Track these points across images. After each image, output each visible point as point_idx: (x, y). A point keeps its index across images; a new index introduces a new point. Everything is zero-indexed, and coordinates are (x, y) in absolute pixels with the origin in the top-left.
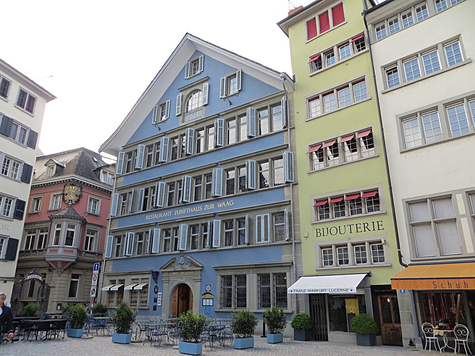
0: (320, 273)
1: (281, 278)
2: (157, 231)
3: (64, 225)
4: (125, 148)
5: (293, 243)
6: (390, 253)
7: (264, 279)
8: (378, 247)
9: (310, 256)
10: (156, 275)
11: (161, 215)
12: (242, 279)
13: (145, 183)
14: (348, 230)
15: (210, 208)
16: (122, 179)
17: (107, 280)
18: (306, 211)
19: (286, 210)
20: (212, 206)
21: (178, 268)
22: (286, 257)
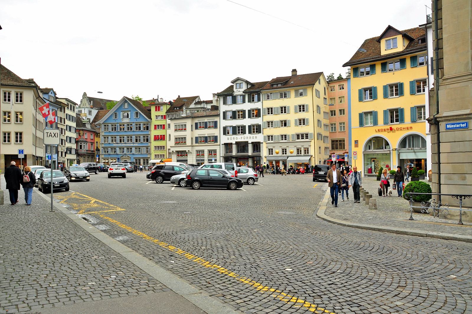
0: (154, 159)
1: (147, 160)
2: (118, 149)
3: (83, 143)
4: (103, 123)
5: (150, 154)
6: (165, 156)
7: (144, 160)
8: (164, 155)
9: (153, 156)
10: (118, 159)
11: (118, 144)
12: (140, 160)
13: (112, 136)
14: (159, 153)
15: (132, 145)
16: (104, 133)
17: (103, 159)
18: (153, 148)
19: (149, 148)
20: (132, 144)
21: (125, 157)
22: (148, 156)
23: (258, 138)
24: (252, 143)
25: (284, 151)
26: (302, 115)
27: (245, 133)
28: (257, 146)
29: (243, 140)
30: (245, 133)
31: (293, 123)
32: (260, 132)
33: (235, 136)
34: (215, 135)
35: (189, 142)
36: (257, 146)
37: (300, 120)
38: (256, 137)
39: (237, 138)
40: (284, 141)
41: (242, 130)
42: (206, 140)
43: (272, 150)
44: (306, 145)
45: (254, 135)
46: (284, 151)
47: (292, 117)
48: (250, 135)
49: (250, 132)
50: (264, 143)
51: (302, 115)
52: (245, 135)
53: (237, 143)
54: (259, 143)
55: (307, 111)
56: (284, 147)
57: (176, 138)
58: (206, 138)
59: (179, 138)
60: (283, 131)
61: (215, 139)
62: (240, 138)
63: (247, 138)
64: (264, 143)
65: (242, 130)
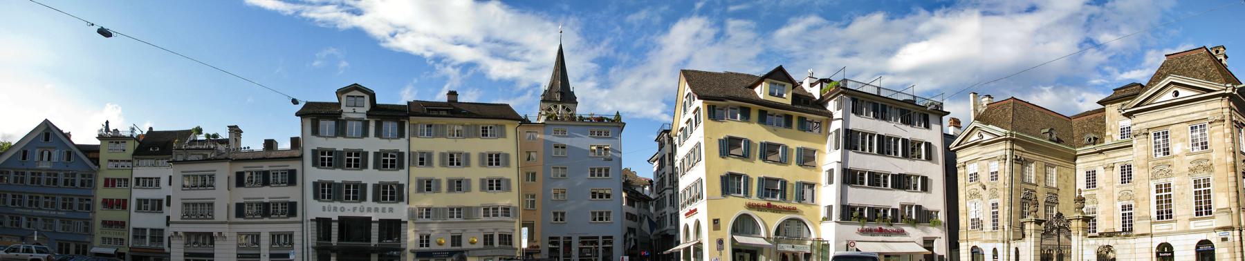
23: (398, 211)
24: (382, 222)
25: (456, 240)
26: (495, 172)
27: (364, 198)
28: (392, 228)
29: (358, 214)
30: (364, 198)
31: (476, 185)
32: (401, 199)
33: (338, 204)
34: (291, 200)
35: (220, 213)
36: (392, 228)
37: (491, 181)
38: (391, 210)
39: (343, 209)
40: (455, 219)
41: (356, 192)
42: (266, 210)
43: (428, 237)
44: (506, 230)
45: (387, 206)
46: (456, 240)
47: (475, 173)
48: (376, 205)
49: (376, 199)
50: (410, 223)
51: (495, 172)
52: (363, 203)
53: (342, 220)
54: (398, 223)
55: (507, 164)
56: (456, 231)
57: (186, 205)
58: (267, 205)
59: (195, 205)
60: (458, 199)
61: (291, 209)
62: (351, 209)
63: (369, 210)
64: (410, 223)
65: (356, 192)
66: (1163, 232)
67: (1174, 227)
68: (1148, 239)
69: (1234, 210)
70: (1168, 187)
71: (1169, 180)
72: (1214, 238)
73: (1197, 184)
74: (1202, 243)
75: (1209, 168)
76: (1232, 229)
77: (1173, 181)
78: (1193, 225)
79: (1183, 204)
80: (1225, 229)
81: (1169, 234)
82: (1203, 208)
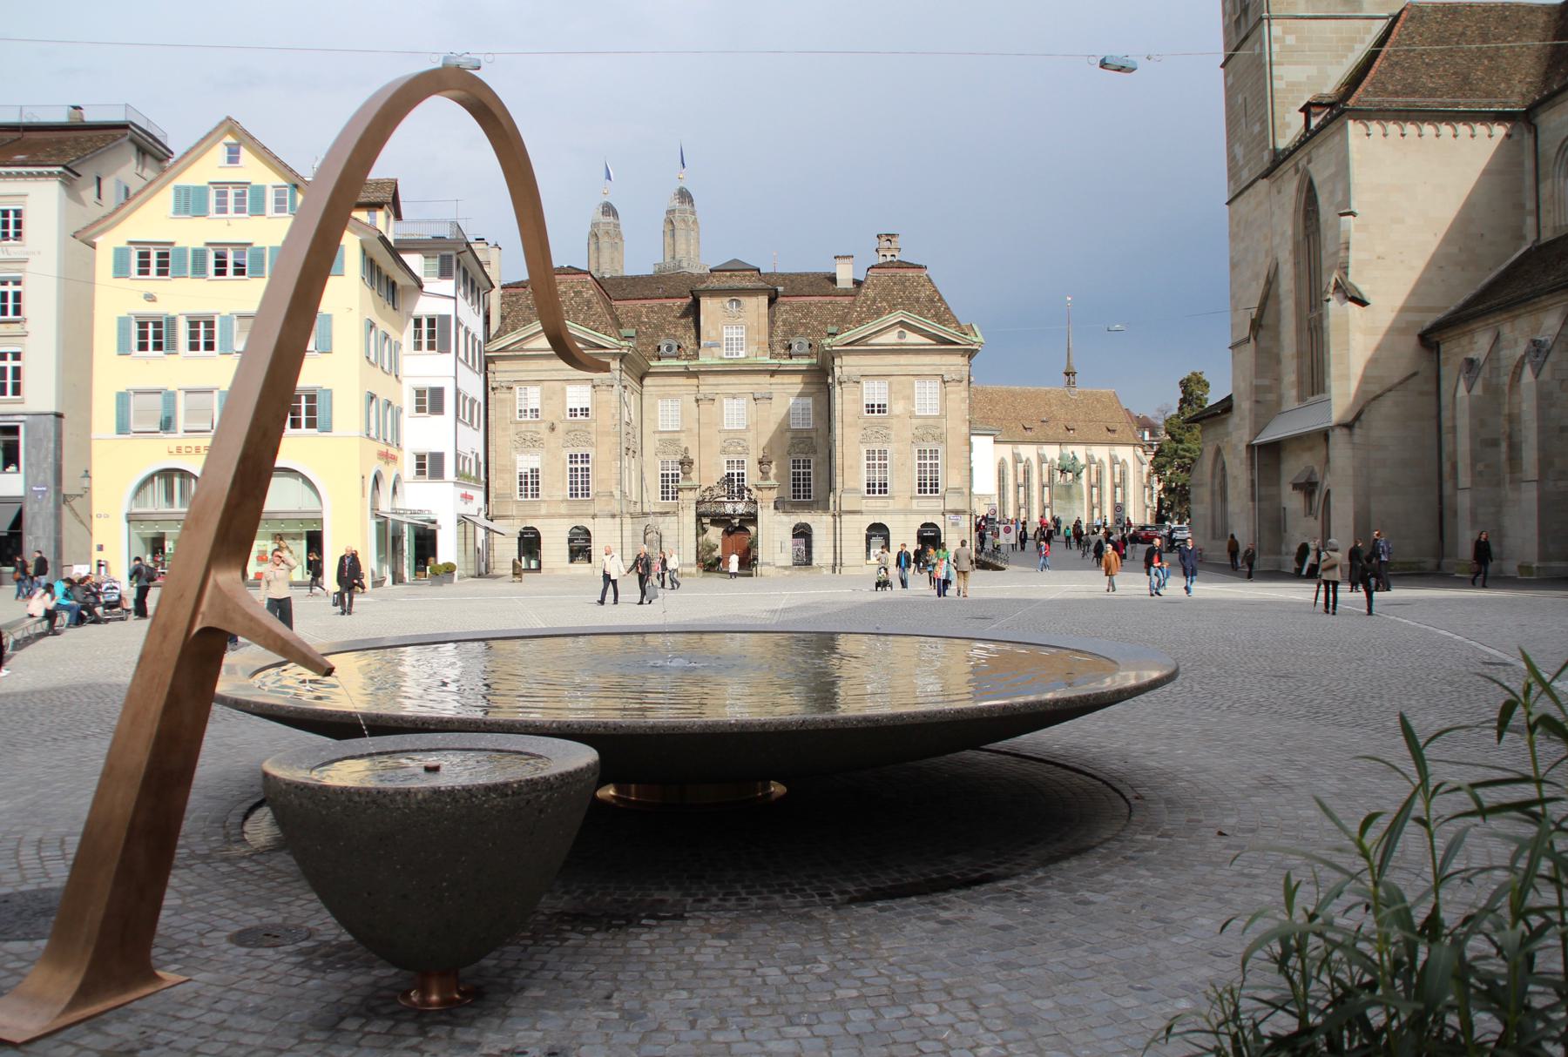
66: (876, 510)
67: (892, 505)
68: (857, 517)
69: (966, 491)
70: (883, 454)
71: (885, 447)
72: (938, 520)
73: (922, 454)
74: (924, 525)
75: (940, 438)
76: (964, 512)
77: (890, 449)
78: (915, 505)
79: (903, 480)
80: (957, 512)
81: (885, 513)
82: (928, 486)
